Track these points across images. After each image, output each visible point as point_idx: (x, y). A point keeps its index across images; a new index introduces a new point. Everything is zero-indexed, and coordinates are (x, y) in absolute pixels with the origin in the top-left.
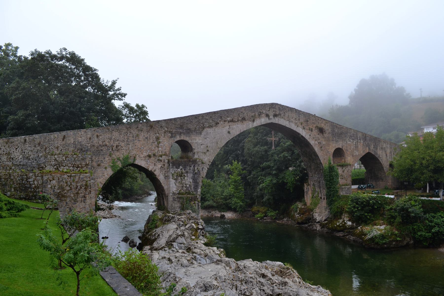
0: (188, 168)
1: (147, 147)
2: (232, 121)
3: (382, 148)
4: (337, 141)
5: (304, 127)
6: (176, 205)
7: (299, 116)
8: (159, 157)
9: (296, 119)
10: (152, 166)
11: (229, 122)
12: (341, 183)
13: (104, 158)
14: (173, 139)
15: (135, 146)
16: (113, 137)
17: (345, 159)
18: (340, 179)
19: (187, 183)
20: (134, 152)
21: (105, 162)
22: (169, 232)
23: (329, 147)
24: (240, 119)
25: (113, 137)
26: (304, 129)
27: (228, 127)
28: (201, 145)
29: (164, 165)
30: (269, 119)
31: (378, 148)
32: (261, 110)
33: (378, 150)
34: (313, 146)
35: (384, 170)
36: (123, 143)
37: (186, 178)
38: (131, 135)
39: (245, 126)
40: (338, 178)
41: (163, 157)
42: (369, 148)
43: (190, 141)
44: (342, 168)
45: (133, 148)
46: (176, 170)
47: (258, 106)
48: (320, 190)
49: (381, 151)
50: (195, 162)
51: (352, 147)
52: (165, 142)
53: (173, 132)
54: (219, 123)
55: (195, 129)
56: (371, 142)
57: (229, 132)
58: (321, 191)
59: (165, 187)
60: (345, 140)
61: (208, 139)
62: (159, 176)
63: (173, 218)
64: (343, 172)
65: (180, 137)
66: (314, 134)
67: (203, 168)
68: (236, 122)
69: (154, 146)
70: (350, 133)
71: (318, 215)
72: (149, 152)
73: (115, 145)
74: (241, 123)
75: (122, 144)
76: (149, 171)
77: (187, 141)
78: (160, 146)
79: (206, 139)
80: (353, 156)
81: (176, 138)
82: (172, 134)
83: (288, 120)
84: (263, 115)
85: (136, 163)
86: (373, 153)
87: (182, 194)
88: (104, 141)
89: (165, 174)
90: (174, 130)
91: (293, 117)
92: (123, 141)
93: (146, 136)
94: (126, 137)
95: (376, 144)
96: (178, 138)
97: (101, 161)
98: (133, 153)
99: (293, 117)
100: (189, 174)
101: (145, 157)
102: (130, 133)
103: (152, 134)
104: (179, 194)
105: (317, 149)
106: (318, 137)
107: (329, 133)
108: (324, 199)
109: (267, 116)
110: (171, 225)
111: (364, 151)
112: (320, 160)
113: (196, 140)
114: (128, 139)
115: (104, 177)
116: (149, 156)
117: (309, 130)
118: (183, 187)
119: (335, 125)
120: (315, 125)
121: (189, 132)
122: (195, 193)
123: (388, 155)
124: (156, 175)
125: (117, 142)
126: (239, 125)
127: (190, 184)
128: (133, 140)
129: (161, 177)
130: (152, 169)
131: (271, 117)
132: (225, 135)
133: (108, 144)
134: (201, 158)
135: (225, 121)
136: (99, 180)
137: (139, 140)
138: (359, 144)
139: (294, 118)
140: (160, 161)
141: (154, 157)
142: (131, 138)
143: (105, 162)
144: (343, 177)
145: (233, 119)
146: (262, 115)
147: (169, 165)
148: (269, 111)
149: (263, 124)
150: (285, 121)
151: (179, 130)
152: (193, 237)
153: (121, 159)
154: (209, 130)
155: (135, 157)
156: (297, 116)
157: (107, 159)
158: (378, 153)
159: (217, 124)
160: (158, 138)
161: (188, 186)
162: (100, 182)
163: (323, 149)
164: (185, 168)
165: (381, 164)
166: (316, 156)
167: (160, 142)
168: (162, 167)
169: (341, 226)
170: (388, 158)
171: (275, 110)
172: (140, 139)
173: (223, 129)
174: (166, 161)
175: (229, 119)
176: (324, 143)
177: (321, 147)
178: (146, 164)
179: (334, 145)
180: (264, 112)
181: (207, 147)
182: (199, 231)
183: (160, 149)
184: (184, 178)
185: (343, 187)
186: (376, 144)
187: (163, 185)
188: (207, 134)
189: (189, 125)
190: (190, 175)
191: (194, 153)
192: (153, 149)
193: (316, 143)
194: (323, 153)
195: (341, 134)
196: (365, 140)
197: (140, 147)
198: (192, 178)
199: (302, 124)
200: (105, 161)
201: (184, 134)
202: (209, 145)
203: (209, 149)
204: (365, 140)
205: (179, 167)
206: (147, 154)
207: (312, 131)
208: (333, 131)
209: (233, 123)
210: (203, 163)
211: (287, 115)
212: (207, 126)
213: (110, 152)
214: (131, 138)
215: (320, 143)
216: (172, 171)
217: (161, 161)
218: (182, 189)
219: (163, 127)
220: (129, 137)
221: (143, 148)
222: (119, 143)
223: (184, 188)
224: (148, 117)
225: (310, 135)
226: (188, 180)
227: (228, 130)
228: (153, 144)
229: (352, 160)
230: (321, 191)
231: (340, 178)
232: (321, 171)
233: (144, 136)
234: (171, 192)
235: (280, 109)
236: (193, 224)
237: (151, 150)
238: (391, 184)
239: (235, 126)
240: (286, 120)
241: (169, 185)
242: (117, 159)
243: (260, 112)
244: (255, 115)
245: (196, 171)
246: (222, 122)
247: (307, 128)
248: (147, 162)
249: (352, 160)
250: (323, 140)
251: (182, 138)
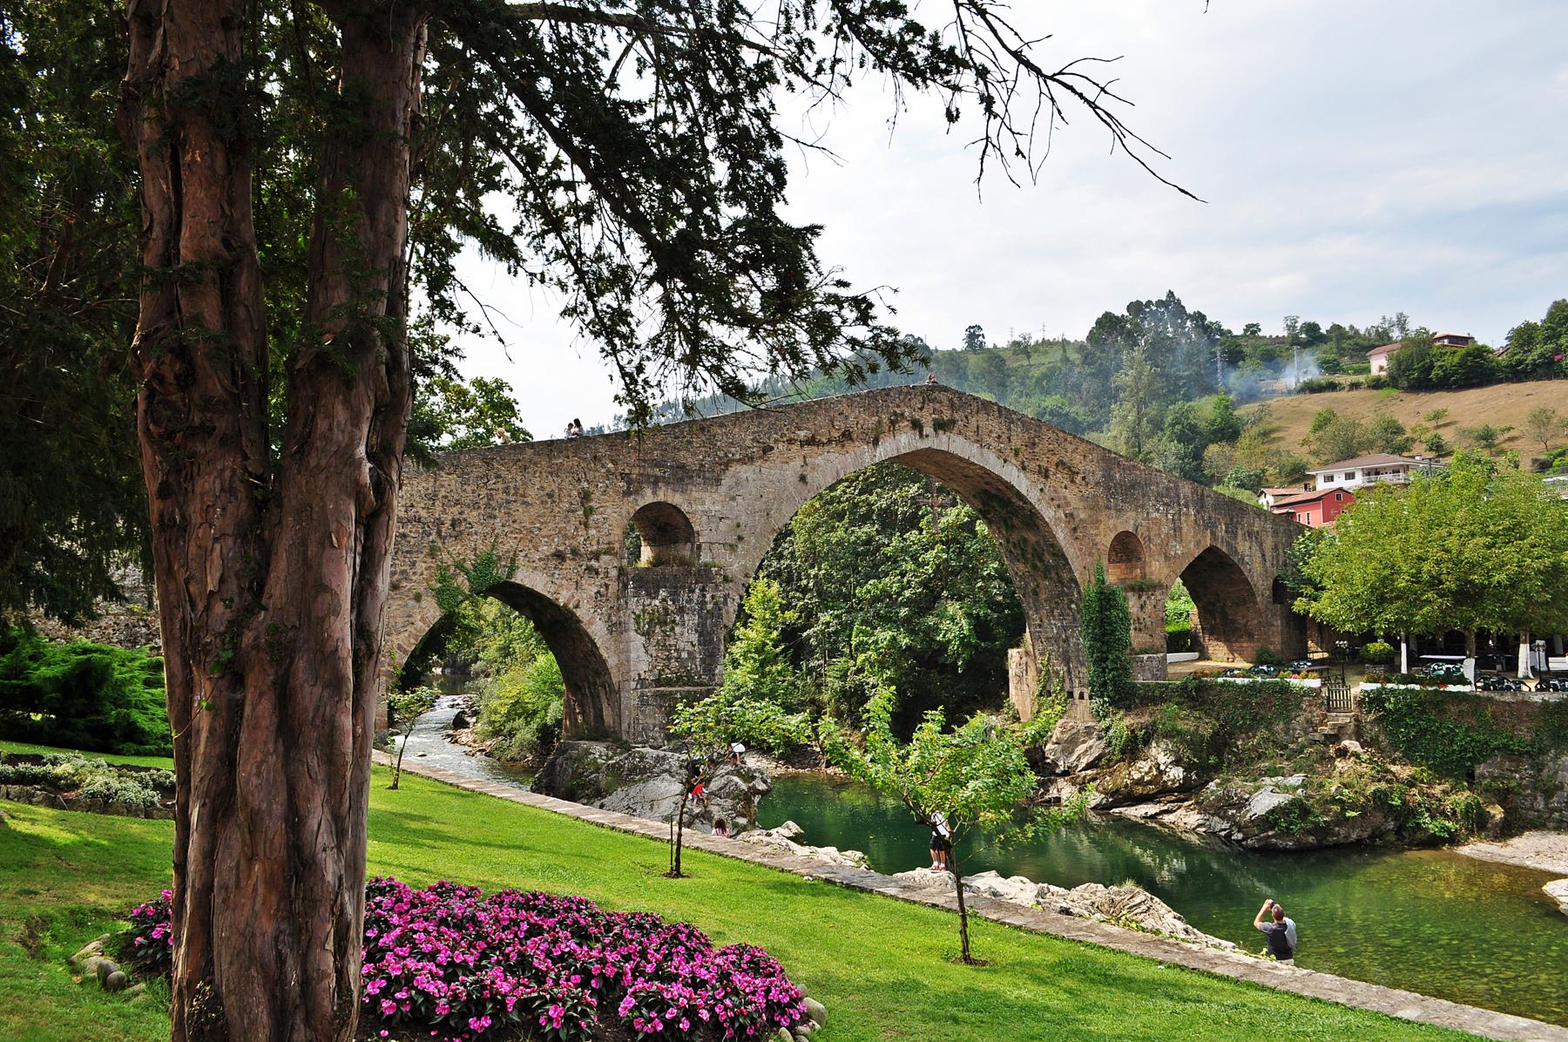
0: (684, 596)
1: (551, 525)
2: (811, 441)
3: (1250, 534)
4: (1120, 510)
5: (1023, 463)
6: (651, 721)
7: (1009, 429)
8: (590, 560)
9: (999, 437)
10: (568, 589)
11: (803, 443)
12: (1135, 645)
13: (413, 564)
14: (631, 498)
15: (514, 522)
16: (443, 493)
17: (1143, 568)
18: (1132, 632)
19: (681, 645)
20: (509, 544)
21: (414, 578)
22: (655, 807)
23: (1097, 528)
24: (836, 434)
25: (443, 493)
26: (1024, 468)
27: (799, 462)
28: (721, 519)
29: (607, 586)
30: (921, 435)
31: (1240, 532)
32: (898, 406)
33: (1240, 537)
34: (1051, 524)
35: (1255, 603)
36: (475, 513)
37: (678, 629)
38: (500, 486)
40: (1128, 630)
41: (604, 558)
42: (1213, 534)
43: (684, 508)
44: (1140, 597)
45: (506, 529)
46: (647, 602)
47: (888, 395)
48: (1069, 668)
49: (1247, 544)
50: (705, 575)
51: (1165, 530)
52: (609, 511)
54: (772, 448)
55: (702, 466)
56: (1220, 514)
57: (803, 479)
58: (1069, 672)
59: (612, 661)
60: (1143, 506)
61: (739, 499)
62: (590, 623)
63: (659, 759)
64: (1142, 607)
65: (654, 493)
67: (726, 597)
68: (824, 444)
69: (574, 521)
70: (1157, 484)
71: (1062, 751)
72: (557, 544)
73: (447, 519)
74: (839, 448)
75: (472, 516)
76: (558, 606)
77: (675, 507)
79: (733, 499)
80: (1167, 558)
81: (643, 496)
82: (629, 483)
85: (518, 582)
86: (1224, 549)
87: (669, 683)
88: (412, 506)
89: (610, 616)
90: (636, 471)
91: (991, 431)
92: (476, 506)
93: (548, 490)
94: (483, 492)
95: (1231, 519)
96: (648, 497)
97: (403, 572)
98: (506, 548)
99: (991, 431)
100: (686, 617)
101: (545, 559)
102: (498, 477)
103: (566, 484)
104: (658, 682)
105: (1061, 535)
106: (1065, 498)
107: (1097, 484)
108: (1081, 696)
109: (917, 425)
110: (658, 782)
111: (1198, 543)
112: (1071, 571)
113: (703, 503)
114: (490, 497)
115: (410, 628)
116: (559, 556)
117: (1040, 472)
118: (669, 658)
120: (1055, 459)
121: (682, 476)
122: (705, 678)
123: (1268, 555)
124: (579, 621)
125: (455, 510)
126: (832, 456)
127: (691, 649)
128: (508, 502)
129: (597, 630)
130: (569, 600)
131: (928, 430)
132: (791, 489)
133: (423, 513)
134: (720, 561)
135: (790, 441)
136: (396, 640)
138: (1183, 518)
140: (593, 575)
141: (574, 559)
142: (500, 496)
143: (414, 578)
144: (1142, 626)
145: (813, 436)
147: (626, 586)
148: (921, 409)
149: (903, 452)
150: (967, 443)
151: (649, 471)
152: (742, 821)
153: (468, 565)
154: (745, 471)
155: (513, 560)
156: (1004, 428)
157: (420, 566)
158: (1240, 549)
159: (767, 449)
160: (586, 496)
161: (684, 655)
162: (400, 647)
163: (1079, 534)
164: (674, 595)
165: (1249, 584)
166: (1060, 555)
167: (589, 512)
168: (598, 592)
169: (1149, 783)
170: (1268, 564)
171: (937, 406)
172: (529, 500)
174: (614, 573)
175: (802, 434)
176: (1082, 516)
177: (1075, 529)
178: (550, 584)
179: (1111, 522)
180: (906, 414)
181: (738, 526)
182: (757, 799)
183: (593, 532)
184: (672, 629)
185: (1145, 657)
186: (1231, 519)
187: (605, 655)
189: (682, 453)
190: (692, 620)
191: (699, 547)
192: (570, 534)
194: (1081, 550)
195: (1133, 486)
196: (1202, 507)
197: (528, 526)
198: (696, 631)
199: (1016, 454)
200: (414, 573)
201: (667, 484)
202: (743, 519)
203: (745, 534)
204: (1202, 507)
205: (657, 593)
206: (553, 551)
207: (1046, 477)
208: (1108, 476)
209: (815, 448)
210: (726, 579)
211: (973, 422)
212: (738, 457)
213: (433, 541)
214: (500, 496)
215: (1072, 515)
216: (634, 605)
217: (597, 573)
218: (667, 667)
219: (600, 460)
220: (494, 492)
222: (460, 513)
223: (674, 664)
224: (517, 423)
225: (1042, 490)
226: (686, 637)
227: (800, 471)
229: (1166, 571)
230: (1069, 672)
231: (1132, 627)
232: (1073, 606)
233: (542, 488)
234: (634, 675)
236: (736, 779)
237: (566, 537)
238: (1279, 647)
239: (819, 460)
241: (624, 652)
242: (457, 567)
243: (895, 413)
244: (879, 422)
245: (710, 606)
246: (780, 445)
247: (1033, 465)
248: (553, 575)
249: (1166, 571)
250: (1081, 505)
251: (661, 497)
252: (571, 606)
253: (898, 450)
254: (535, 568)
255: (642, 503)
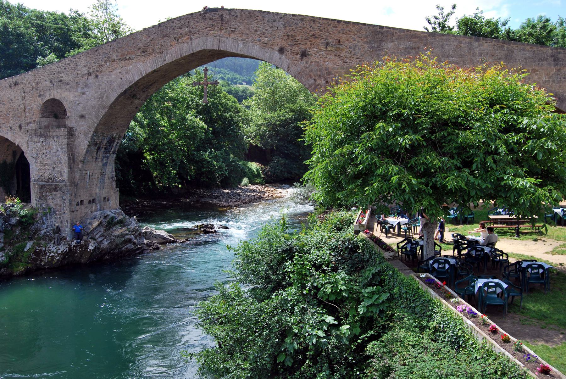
14: (40, 99)
39: (149, 65)
43: (62, 100)
47: (173, 22)
53: (42, 88)
54: (102, 66)
62: (26, 153)
65: (50, 95)
66: (315, 62)
74: (142, 58)
78: (27, 110)
79: (84, 94)
83: (242, 40)
84: (185, 38)
91: (256, 31)
99: (256, 31)
106: (326, 69)
119: (387, 31)
137: (3, 104)
139: (259, 33)
146: (183, 39)
154: (91, 79)
173: (111, 73)
183: (27, 114)
188: (85, 86)
192: (19, 115)
193: (319, 82)
197: (6, 113)
221: (9, 114)
228: (18, 107)
235: (222, 19)
240: (240, 39)
246: (108, 64)
252: (20, 145)
253: (181, 55)
254: (8, 130)
255: (45, 100)
